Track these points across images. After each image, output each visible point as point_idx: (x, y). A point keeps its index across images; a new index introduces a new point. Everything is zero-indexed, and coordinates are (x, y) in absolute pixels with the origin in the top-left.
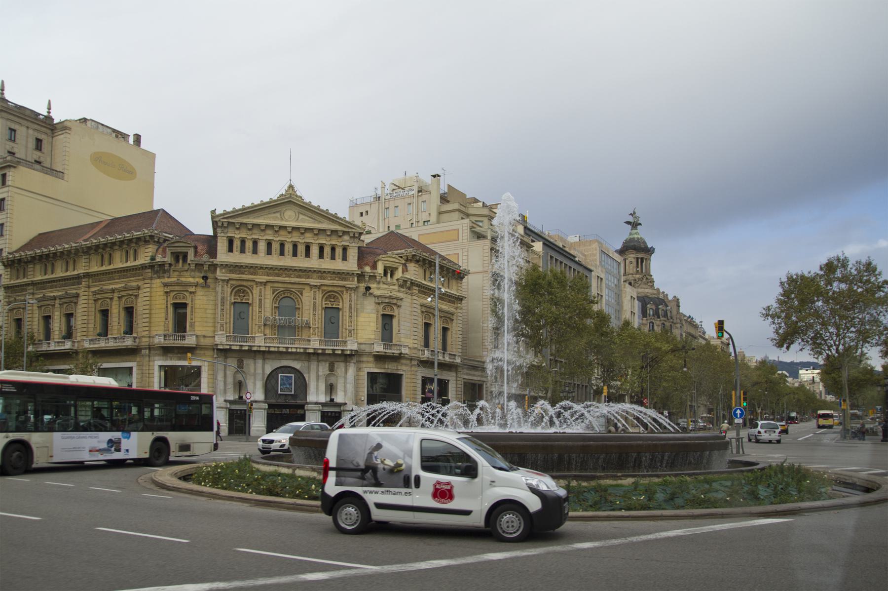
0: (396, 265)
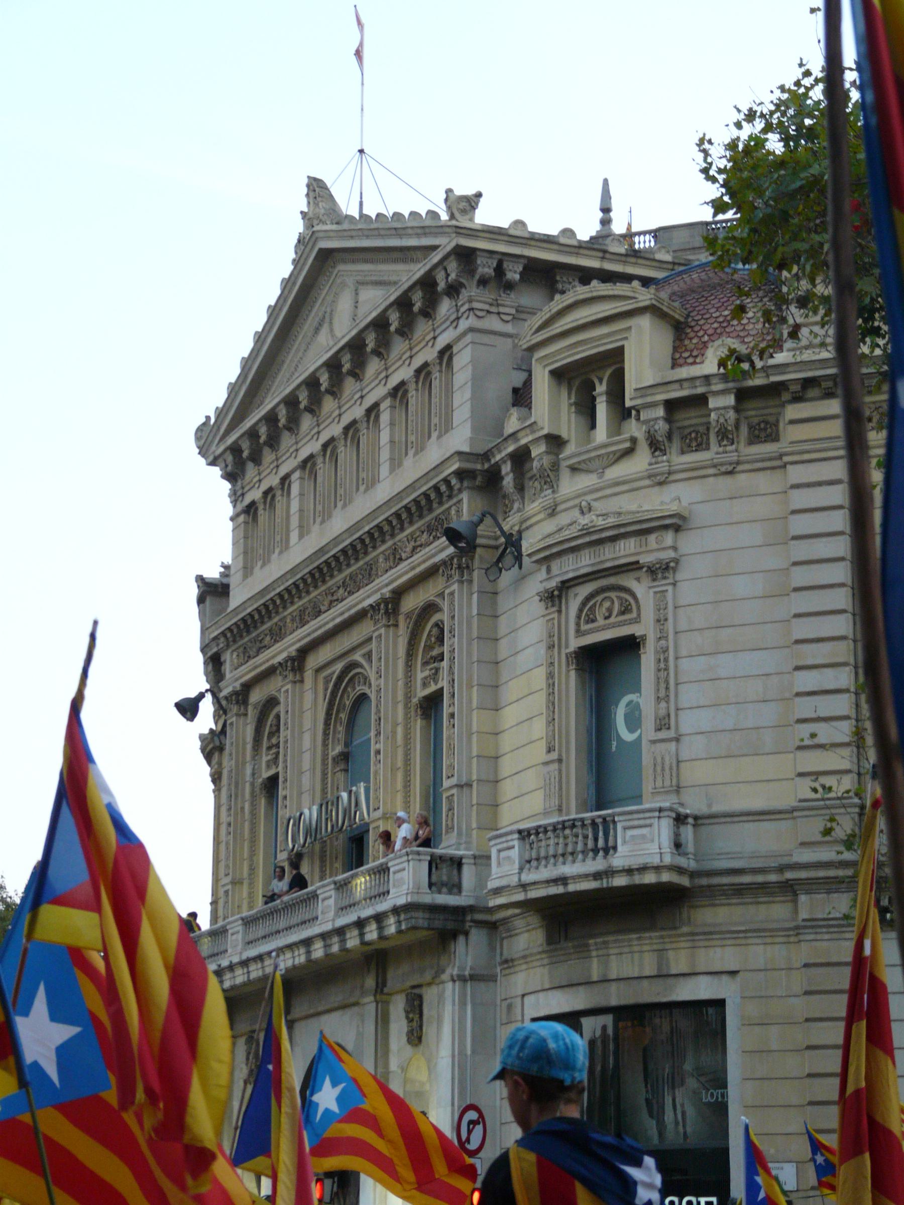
0: (597, 341)
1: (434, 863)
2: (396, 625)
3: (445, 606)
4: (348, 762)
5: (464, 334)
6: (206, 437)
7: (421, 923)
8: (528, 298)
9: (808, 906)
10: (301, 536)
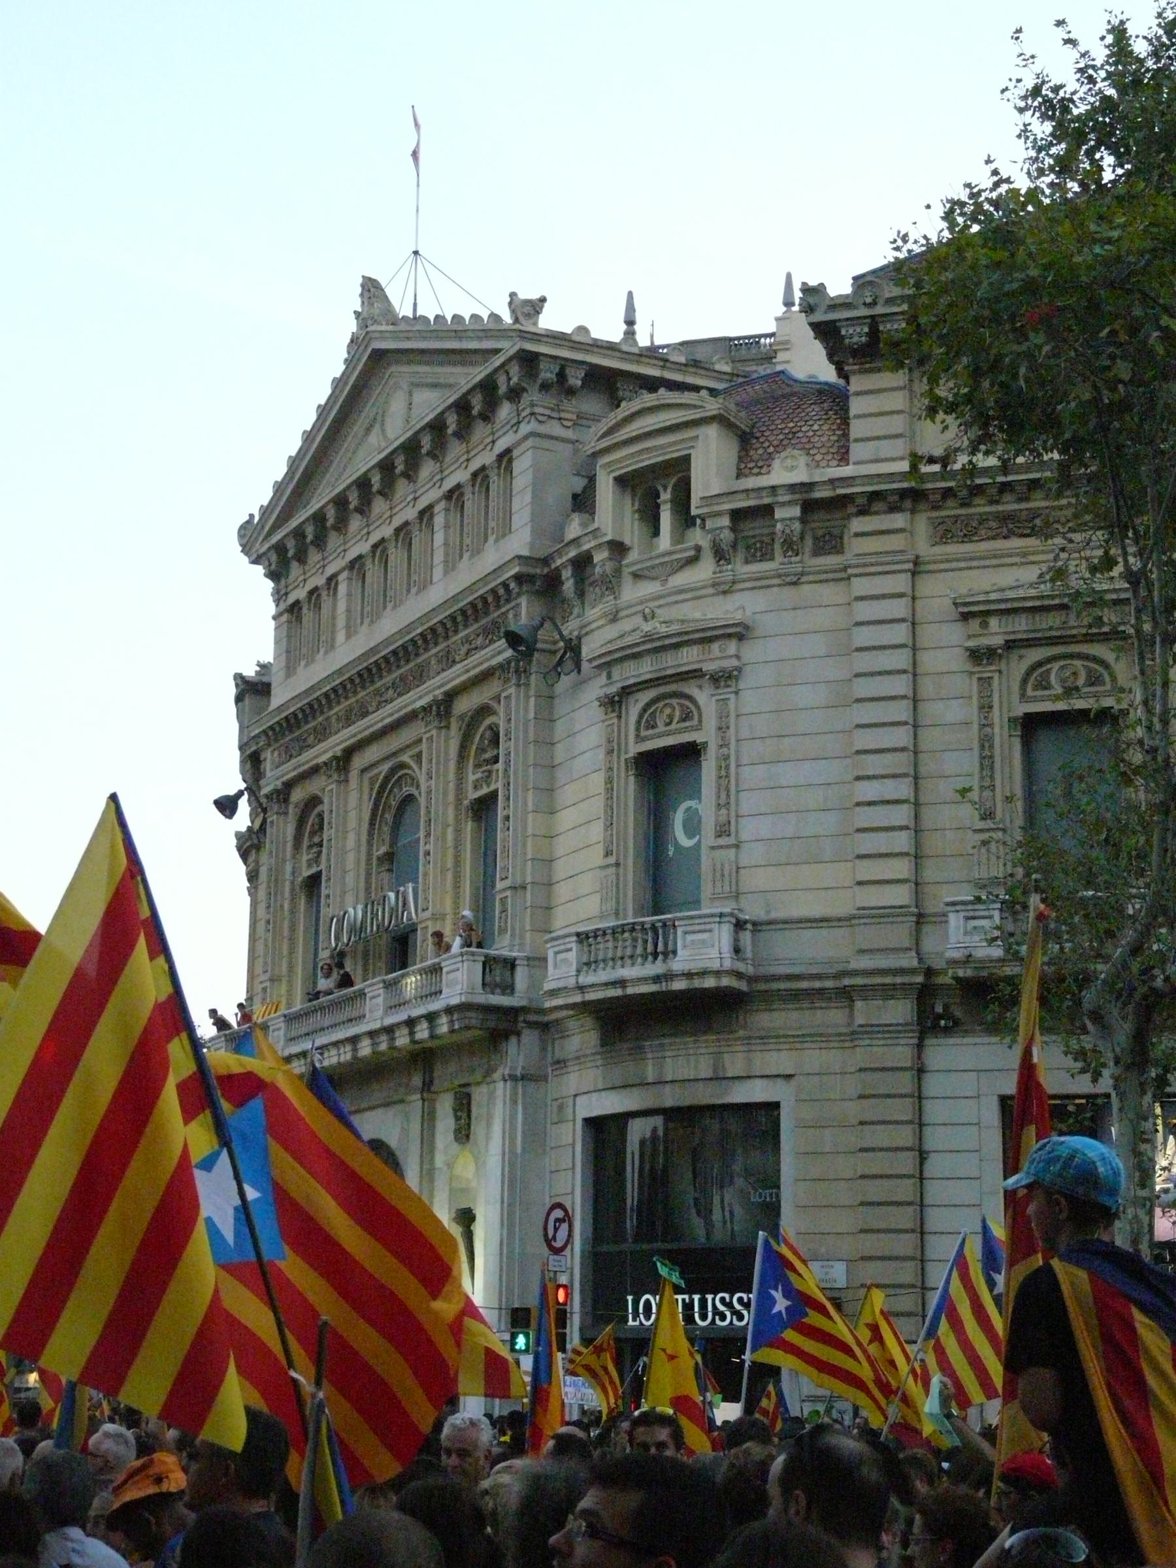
1: (489, 963)
2: (448, 727)
3: (501, 710)
4: (394, 861)
5: (526, 438)
6: (252, 538)
7: (474, 1022)
8: (591, 404)
9: (863, 1012)
10: (348, 636)
